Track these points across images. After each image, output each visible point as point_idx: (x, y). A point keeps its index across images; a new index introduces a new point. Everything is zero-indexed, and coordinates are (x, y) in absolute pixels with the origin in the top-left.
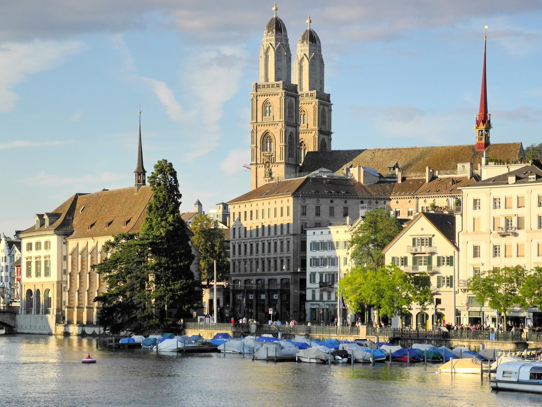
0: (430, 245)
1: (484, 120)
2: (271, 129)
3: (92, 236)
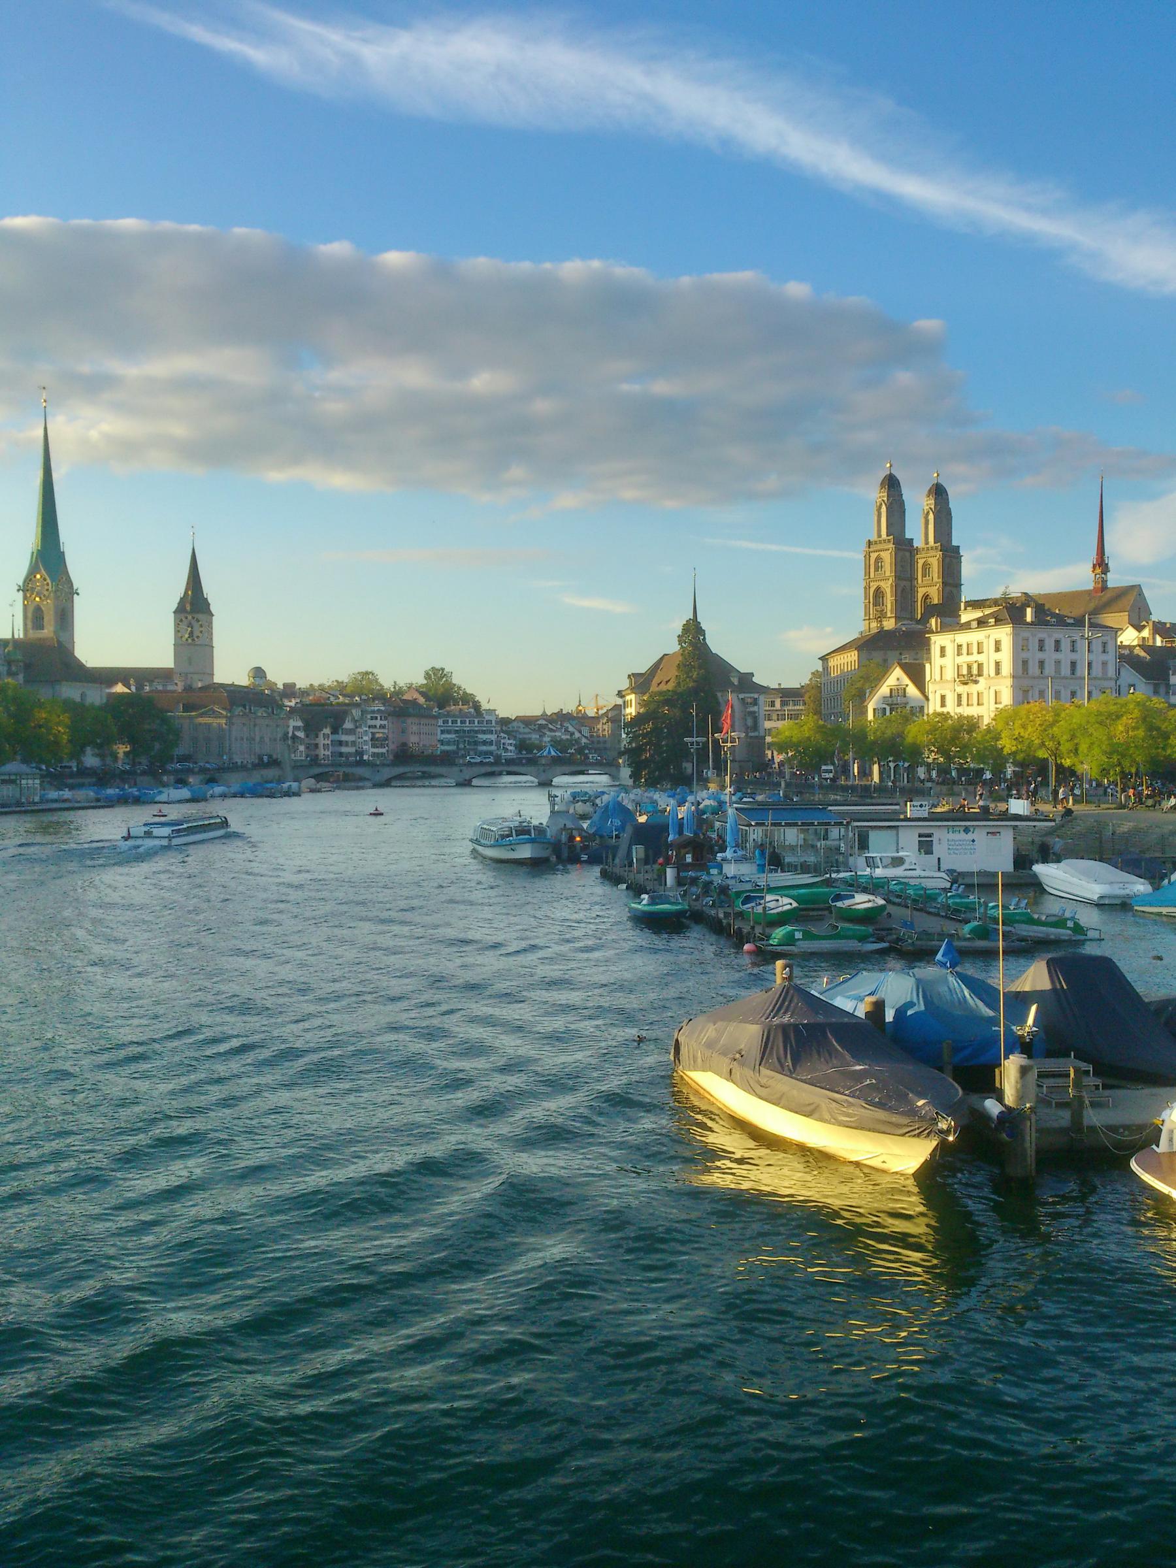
2: (882, 584)
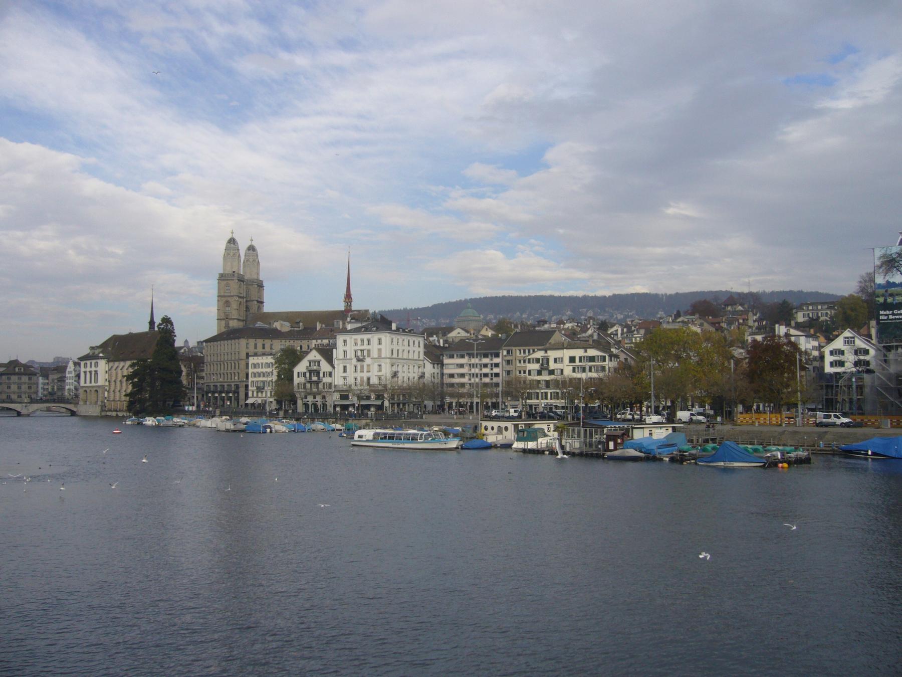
0: (319, 365)
1: (348, 296)
3: (124, 360)
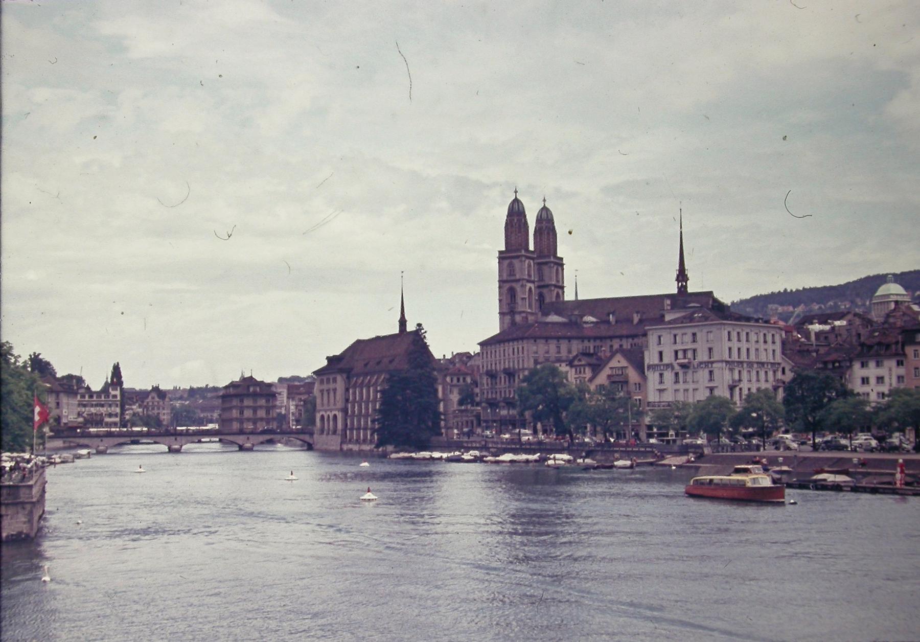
1: (682, 276)
